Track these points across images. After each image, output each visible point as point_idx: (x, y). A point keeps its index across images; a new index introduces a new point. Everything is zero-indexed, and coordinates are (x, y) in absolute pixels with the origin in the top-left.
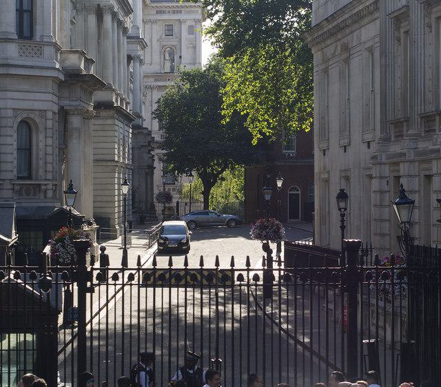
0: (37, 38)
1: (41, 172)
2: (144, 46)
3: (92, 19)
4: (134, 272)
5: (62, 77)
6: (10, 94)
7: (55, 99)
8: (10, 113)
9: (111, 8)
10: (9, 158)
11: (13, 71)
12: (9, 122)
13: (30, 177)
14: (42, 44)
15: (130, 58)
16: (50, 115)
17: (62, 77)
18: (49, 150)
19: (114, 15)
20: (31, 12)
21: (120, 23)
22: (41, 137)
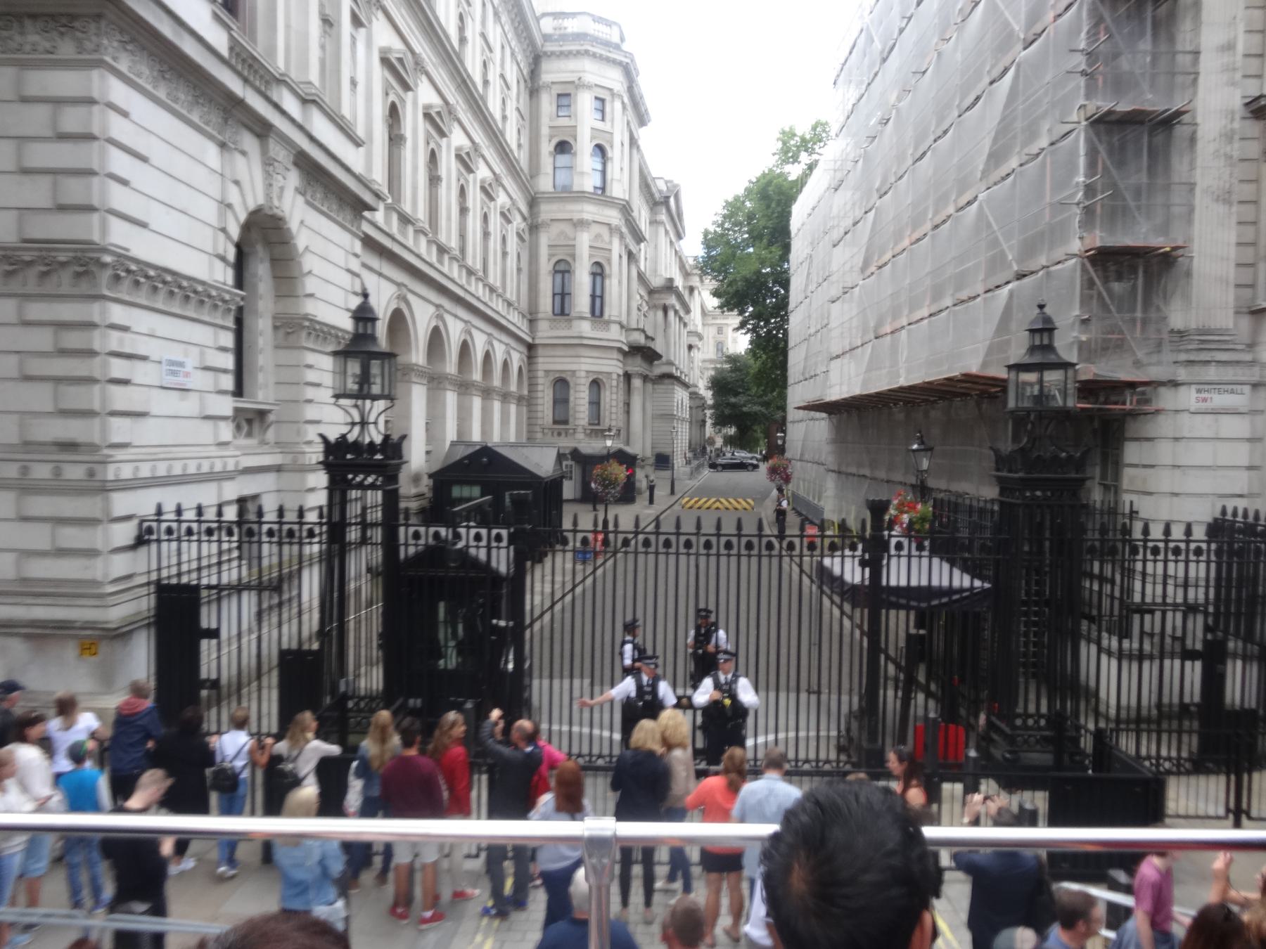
0: (606, 316)
1: (607, 420)
2: (700, 337)
3: (660, 314)
4: (630, 536)
5: (626, 349)
6: (583, 360)
7: (620, 365)
8: (583, 374)
9: (673, 307)
10: (582, 409)
11: (585, 342)
12: (583, 381)
13: (599, 424)
14: (608, 323)
15: (690, 347)
16: (615, 376)
17: (626, 349)
18: (614, 403)
19: (676, 312)
20: (602, 297)
21: (681, 318)
22: (608, 393)
